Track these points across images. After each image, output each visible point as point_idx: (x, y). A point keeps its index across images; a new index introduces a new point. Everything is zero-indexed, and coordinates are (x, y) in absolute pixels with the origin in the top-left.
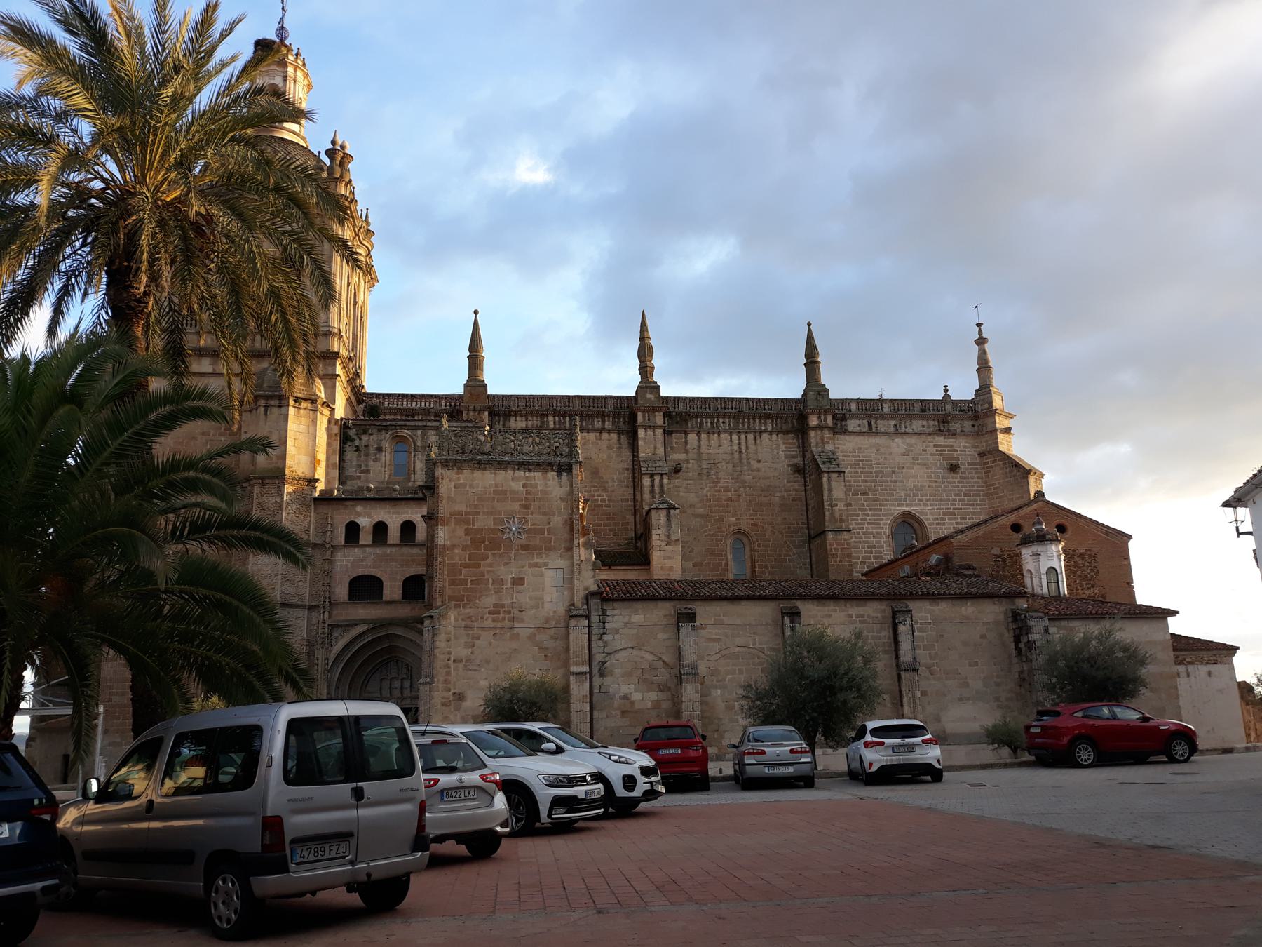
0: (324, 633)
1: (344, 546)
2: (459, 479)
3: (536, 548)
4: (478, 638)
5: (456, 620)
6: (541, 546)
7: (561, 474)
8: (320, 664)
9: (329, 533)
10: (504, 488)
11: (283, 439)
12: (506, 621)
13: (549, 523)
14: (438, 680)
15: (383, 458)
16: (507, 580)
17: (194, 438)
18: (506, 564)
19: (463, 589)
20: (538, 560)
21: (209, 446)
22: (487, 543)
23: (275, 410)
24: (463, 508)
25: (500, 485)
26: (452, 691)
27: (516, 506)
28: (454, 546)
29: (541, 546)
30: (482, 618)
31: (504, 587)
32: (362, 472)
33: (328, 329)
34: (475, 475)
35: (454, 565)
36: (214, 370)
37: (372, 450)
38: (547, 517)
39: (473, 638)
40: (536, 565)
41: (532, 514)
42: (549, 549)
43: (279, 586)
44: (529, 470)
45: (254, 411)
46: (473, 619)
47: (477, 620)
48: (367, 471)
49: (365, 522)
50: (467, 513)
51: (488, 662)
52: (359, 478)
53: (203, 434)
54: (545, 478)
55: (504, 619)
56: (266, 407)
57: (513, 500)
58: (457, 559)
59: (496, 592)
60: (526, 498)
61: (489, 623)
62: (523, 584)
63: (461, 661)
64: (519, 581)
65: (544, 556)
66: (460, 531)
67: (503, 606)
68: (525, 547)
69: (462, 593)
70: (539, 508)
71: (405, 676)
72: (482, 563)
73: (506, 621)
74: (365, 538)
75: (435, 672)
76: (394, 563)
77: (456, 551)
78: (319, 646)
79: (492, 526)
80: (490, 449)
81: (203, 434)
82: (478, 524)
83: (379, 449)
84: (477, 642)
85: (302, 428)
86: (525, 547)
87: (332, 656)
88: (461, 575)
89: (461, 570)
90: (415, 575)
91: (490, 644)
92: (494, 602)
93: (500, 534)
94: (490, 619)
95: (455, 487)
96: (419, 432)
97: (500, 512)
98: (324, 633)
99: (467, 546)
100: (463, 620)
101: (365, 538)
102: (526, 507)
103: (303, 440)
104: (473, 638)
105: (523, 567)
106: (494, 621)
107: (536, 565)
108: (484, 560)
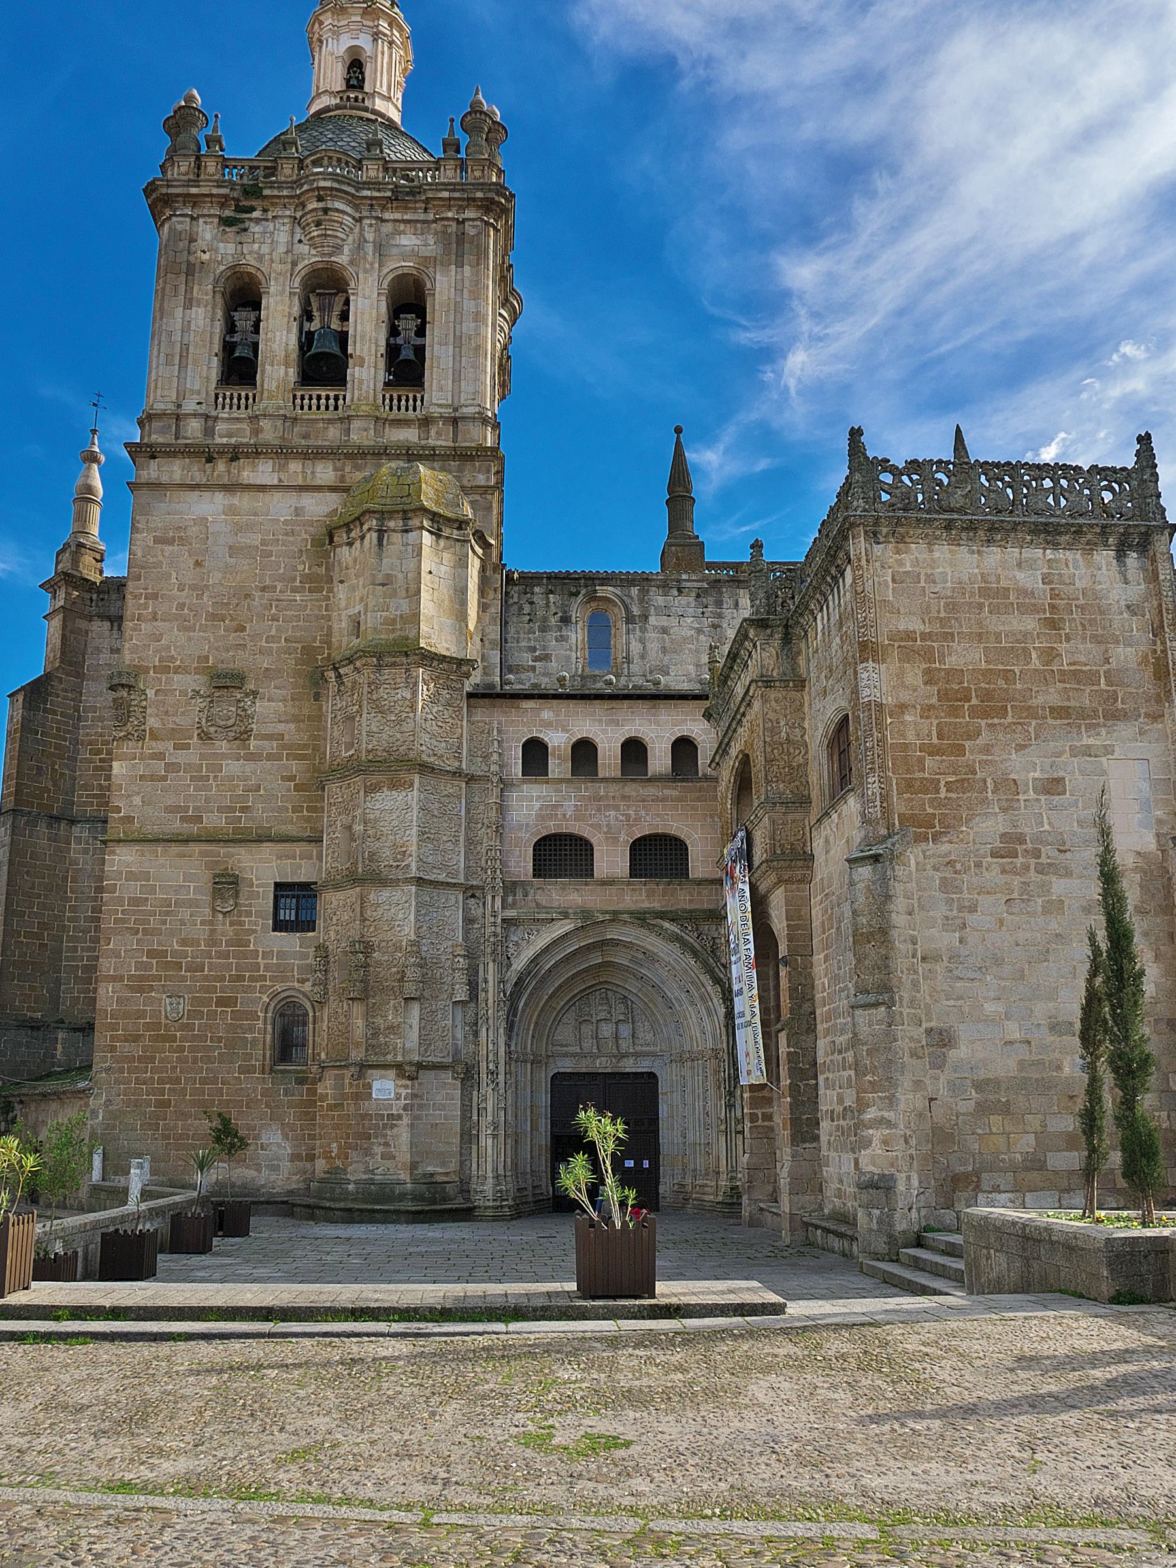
0: (495, 935)
1: (524, 782)
2: (900, 563)
3: (1082, 714)
4: (973, 909)
5: (920, 867)
6: (1095, 711)
7: (1125, 555)
8: (491, 990)
9: (495, 757)
10: (1003, 584)
11: (413, 587)
12: (1032, 872)
13: (1107, 661)
14: (901, 998)
15: (574, 636)
16: (1027, 784)
17: (247, 596)
18: (1020, 747)
19: (931, 801)
20: (1091, 741)
21: (273, 611)
22: (974, 701)
23: (396, 538)
24: (916, 625)
25: (993, 578)
26: (924, 1025)
27: (1030, 624)
28: (902, 707)
29: (1095, 711)
30: (978, 865)
31: (1021, 797)
32: (536, 659)
33: (477, 409)
34: (936, 555)
35: (905, 747)
36: (280, 480)
37: (553, 621)
38: (1103, 647)
39: (961, 909)
40: (1087, 751)
41: (1068, 640)
42: (1114, 716)
43: (414, 848)
44: (1056, 546)
45: (358, 544)
46: (958, 866)
47: (966, 870)
48: (546, 658)
49: (558, 740)
50: (925, 636)
51: (998, 961)
52: (533, 668)
53: (263, 589)
54: (1089, 564)
55: (1026, 868)
56: (381, 532)
57: (1024, 609)
58: (911, 737)
59: (1004, 810)
60: (1053, 607)
61: (992, 875)
62: (1064, 793)
63: (937, 958)
64: (1053, 786)
65: (1103, 731)
66: (914, 675)
67: (1021, 839)
68: (1059, 712)
69: (930, 810)
70: (1083, 625)
71: (622, 1017)
72: (967, 744)
73: (1032, 872)
74: (558, 766)
75: (895, 982)
76: (613, 813)
77: (908, 718)
78: (489, 959)
79: (984, 665)
80: (961, 502)
81: (263, 589)
82: (952, 662)
83: (565, 620)
84: (971, 919)
85: (444, 570)
86: (1059, 712)
87: (512, 976)
88: (923, 770)
89: (921, 761)
90: (650, 836)
91: (1001, 922)
92: (1002, 830)
93: (1001, 683)
94: (996, 870)
95: (894, 581)
96: (635, 591)
97: (998, 635)
98: (495, 935)
99: (931, 707)
100: (936, 869)
101: (558, 766)
102: (1053, 624)
103: (445, 592)
104: (961, 909)
105: (1059, 755)
106: (1004, 872)
107: (1087, 751)
108: (969, 738)
